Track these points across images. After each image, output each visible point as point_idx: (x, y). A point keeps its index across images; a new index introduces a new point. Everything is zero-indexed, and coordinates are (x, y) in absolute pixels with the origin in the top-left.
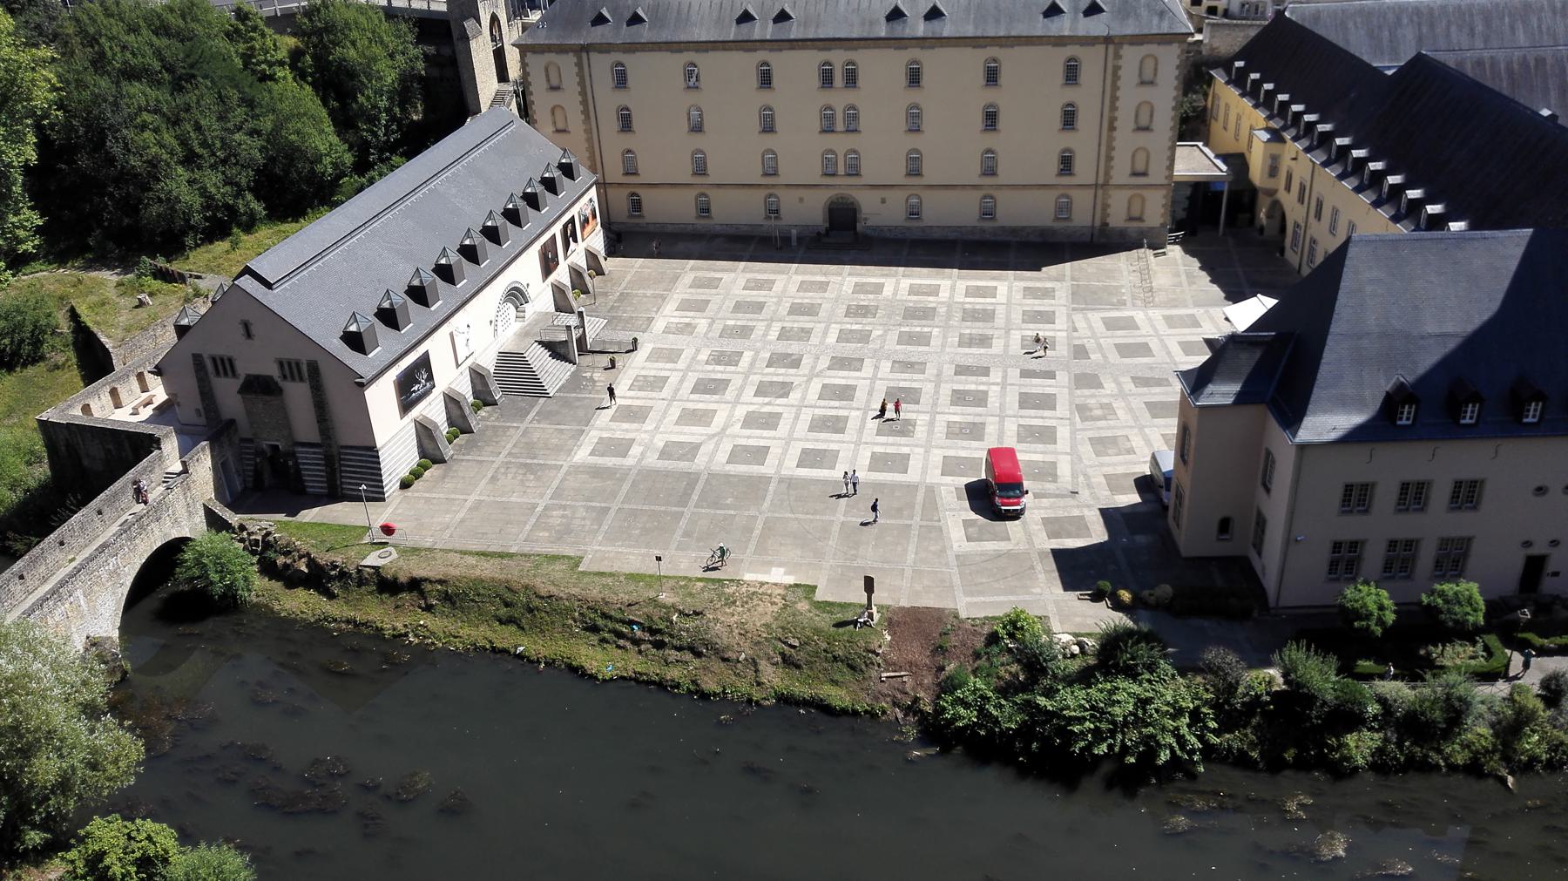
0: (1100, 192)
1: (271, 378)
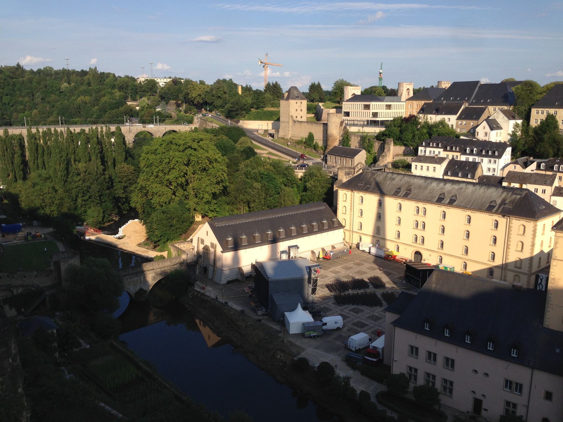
0: (503, 271)
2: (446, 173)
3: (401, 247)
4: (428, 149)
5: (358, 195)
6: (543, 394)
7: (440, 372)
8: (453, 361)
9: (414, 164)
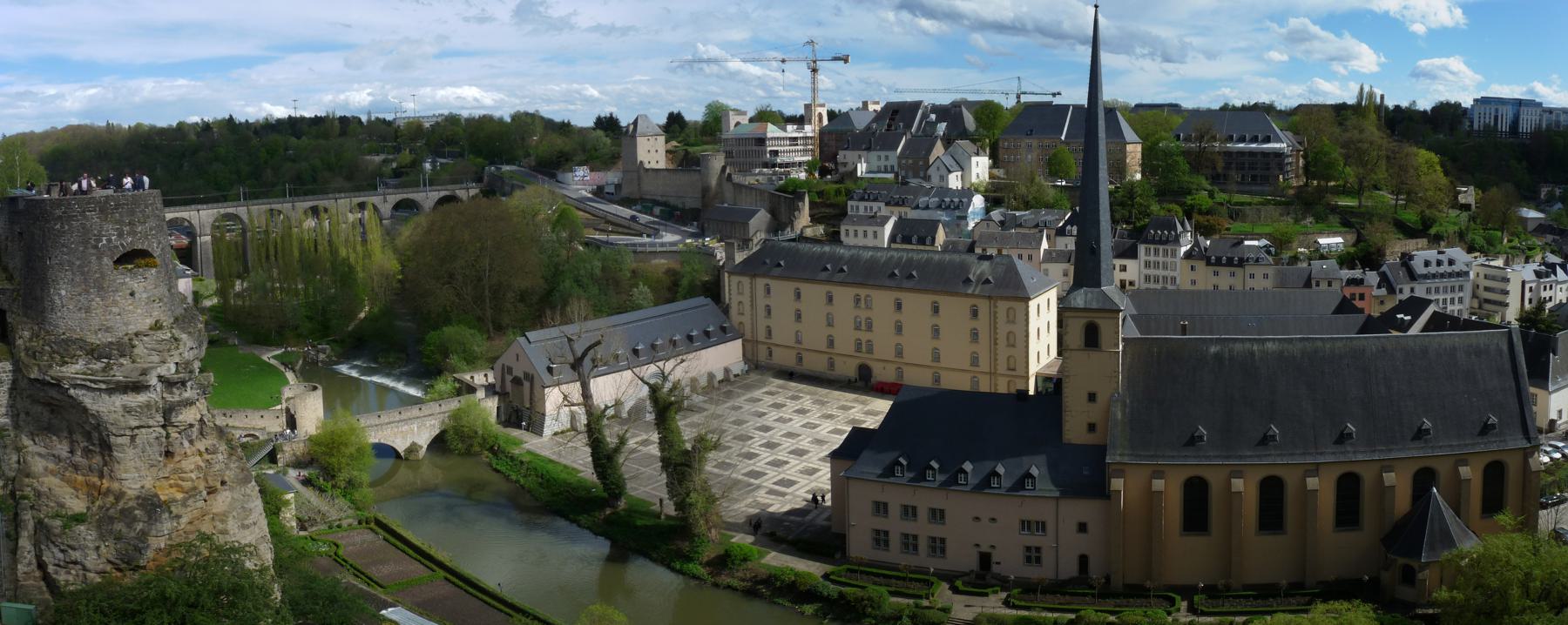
2: (893, 239)
3: (838, 361)
4: (862, 205)
5: (761, 283)
6: (1075, 528)
7: (923, 529)
8: (942, 512)
9: (843, 229)
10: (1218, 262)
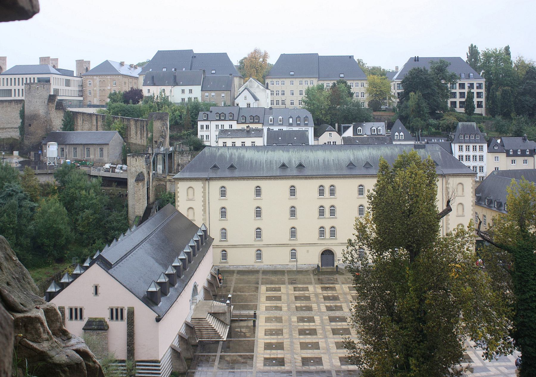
1: (104, 319)
5: (215, 186)
10: (515, 154)
